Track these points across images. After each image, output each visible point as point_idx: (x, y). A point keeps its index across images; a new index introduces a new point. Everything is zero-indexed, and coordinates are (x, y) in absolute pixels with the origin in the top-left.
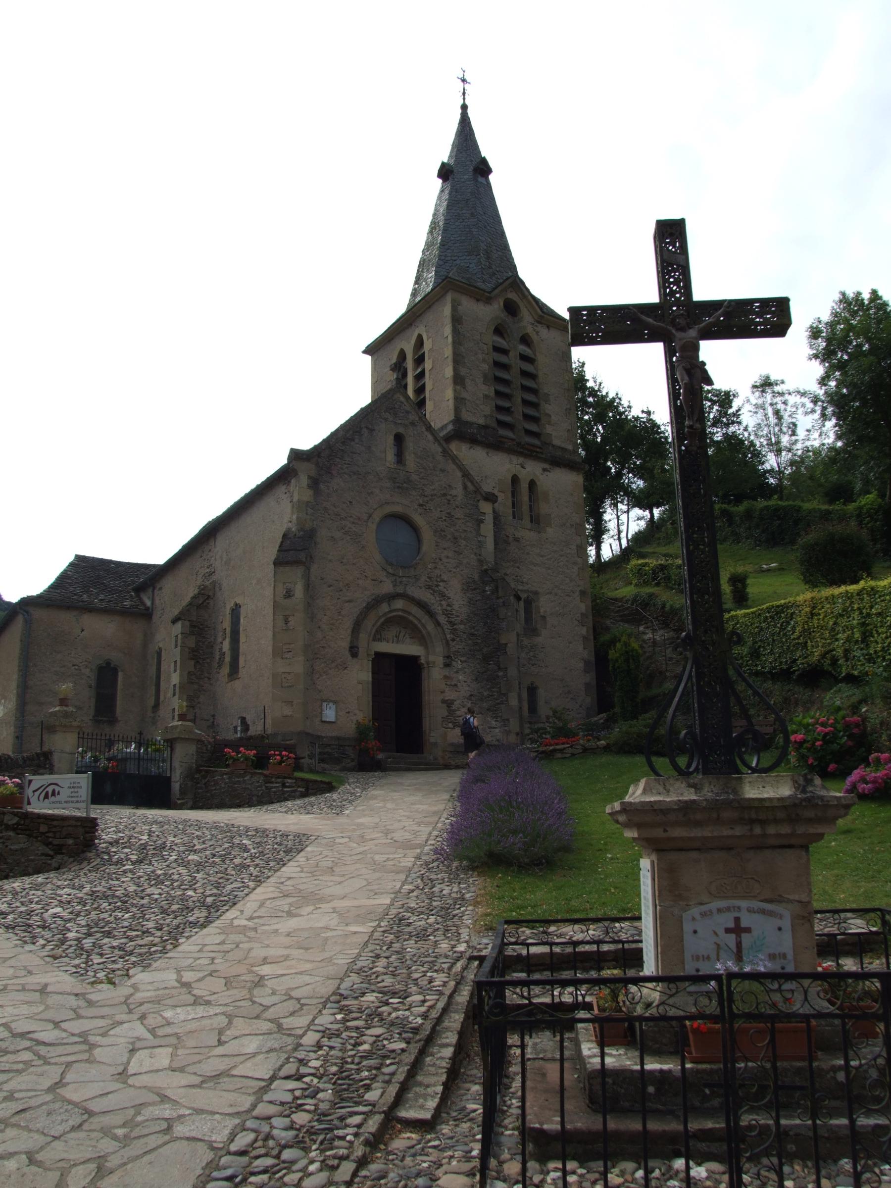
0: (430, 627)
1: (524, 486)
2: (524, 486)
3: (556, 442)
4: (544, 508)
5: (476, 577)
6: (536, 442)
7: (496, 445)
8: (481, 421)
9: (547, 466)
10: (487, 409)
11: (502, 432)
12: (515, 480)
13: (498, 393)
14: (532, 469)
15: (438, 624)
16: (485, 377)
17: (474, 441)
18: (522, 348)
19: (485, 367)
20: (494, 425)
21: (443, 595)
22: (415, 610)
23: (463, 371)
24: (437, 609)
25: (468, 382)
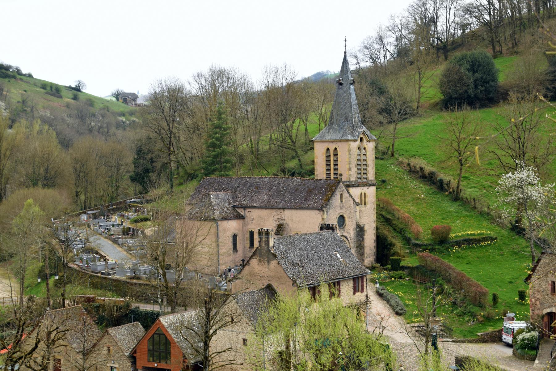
0: (347, 242)
1: (363, 195)
2: (363, 195)
3: (370, 179)
4: (367, 200)
5: (355, 226)
6: (365, 180)
7: (359, 185)
8: (354, 179)
9: (368, 187)
10: (356, 175)
11: (359, 180)
12: (361, 194)
13: (358, 169)
14: (365, 190)
15: (348, 241)
16: (356, 165)
17: (353, 186)
18: (364, 151)
19: (355, 162)
20: (357, 179)
21: (349, 233)
22: (345, 239)
23: (351, 166)
24: (348, 237)
25: (352, 169)
